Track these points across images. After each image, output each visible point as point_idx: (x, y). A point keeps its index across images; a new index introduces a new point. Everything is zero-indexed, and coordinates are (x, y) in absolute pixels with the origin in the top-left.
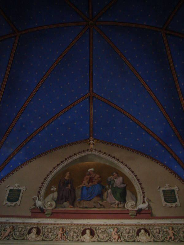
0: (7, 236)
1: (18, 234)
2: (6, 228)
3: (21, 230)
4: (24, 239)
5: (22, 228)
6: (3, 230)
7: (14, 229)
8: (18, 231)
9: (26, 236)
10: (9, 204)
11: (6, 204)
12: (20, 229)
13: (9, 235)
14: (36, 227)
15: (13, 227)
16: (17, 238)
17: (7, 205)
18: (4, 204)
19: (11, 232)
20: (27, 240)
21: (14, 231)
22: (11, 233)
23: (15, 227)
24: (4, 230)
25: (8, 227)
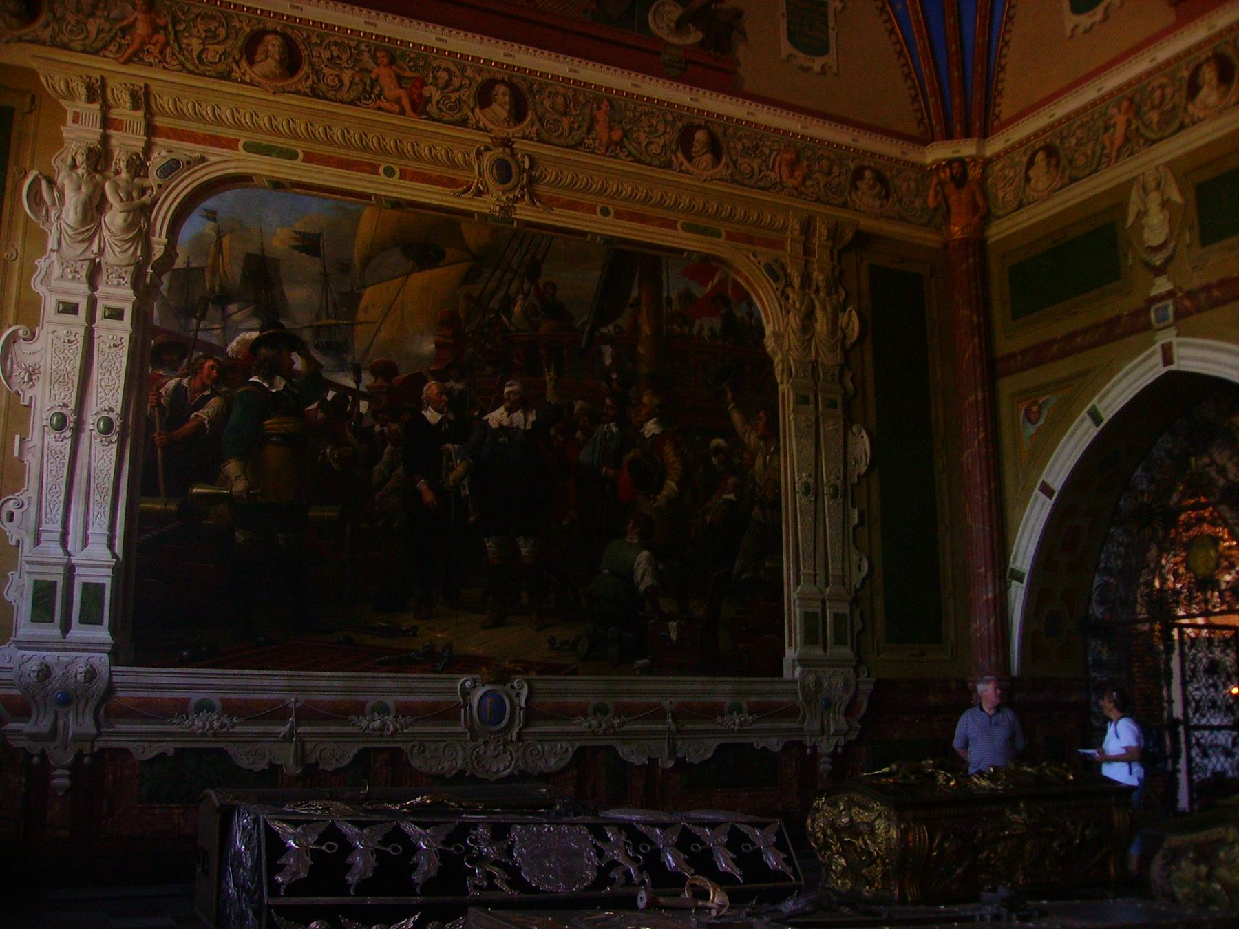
0: (1123, 146)
1: (1154, 117)
2: (1110, 119)
3: (1163, 97)
4: (1182, 127)
5: (1162, 87)
6: (1101, 131)
7: (1135, 109)
8: (1153, 107)
9: (1185, 108)
10: (1084, 20)
11: (1076, 26)
12: (1157, 94)
13: (1127, 139)
14: (1210, 54)
15: (1131, 100)
16: (1159, 135)
17: (1080, 30)
18: (1068, 33)
19: (1129, 123)
20: (1194, 123)
21: (1137, 114)
22: (1133, 127)
23: (1137, 98)
24: (1107, 129)
25: (1115, 111)
